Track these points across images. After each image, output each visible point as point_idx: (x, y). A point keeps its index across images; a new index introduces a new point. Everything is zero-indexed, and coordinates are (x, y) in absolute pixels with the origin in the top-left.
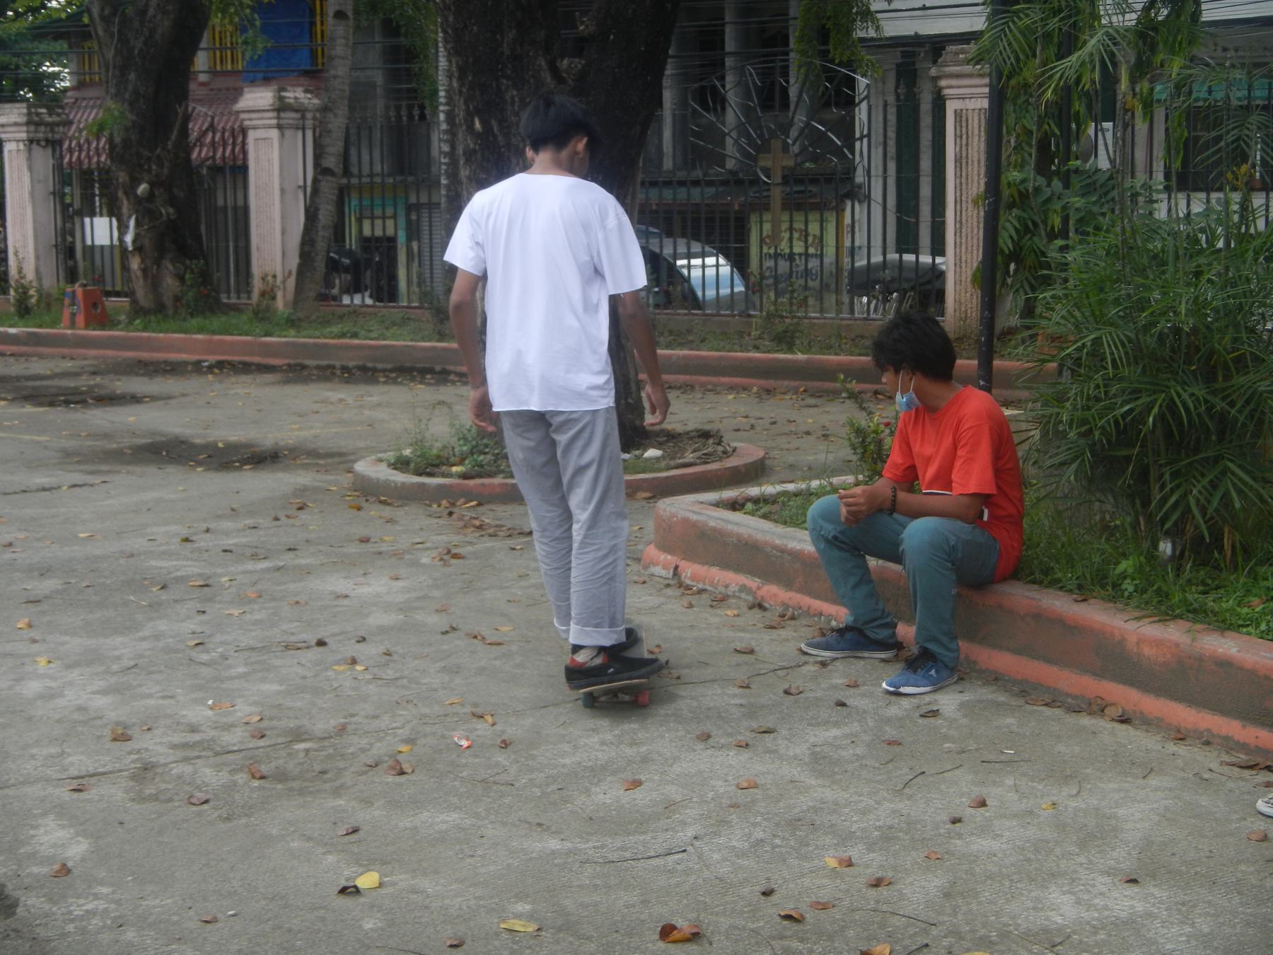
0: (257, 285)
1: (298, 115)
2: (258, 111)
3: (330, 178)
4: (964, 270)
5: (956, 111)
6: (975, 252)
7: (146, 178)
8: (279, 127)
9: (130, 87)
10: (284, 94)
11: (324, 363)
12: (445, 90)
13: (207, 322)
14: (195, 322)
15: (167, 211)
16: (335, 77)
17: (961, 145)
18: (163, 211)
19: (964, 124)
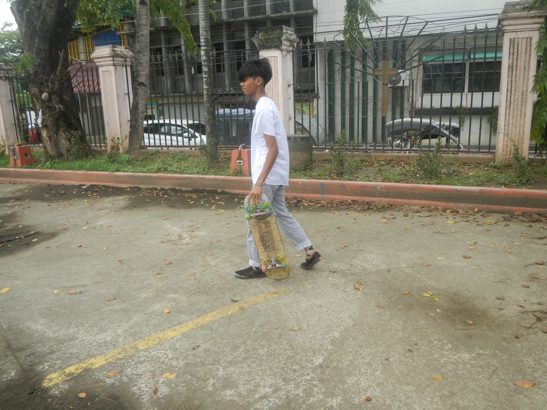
0: (109, 143)
1: (123, 60)
2: (103, 57)
3: (143, 87)
4: (510, 128)
5: (511, 39)
6: (519, 118)
7: (46, 90)
8: (114, 65)
9: (36, 46)
10: (115, 49)
11: (151, 187)
12: (204, 38)
13: (84, 163)
14: (77, 163)
15: (59, 107)
16: (142, 35)
17: (513, 58)
18: (57, 107)
19: (516, 46)
